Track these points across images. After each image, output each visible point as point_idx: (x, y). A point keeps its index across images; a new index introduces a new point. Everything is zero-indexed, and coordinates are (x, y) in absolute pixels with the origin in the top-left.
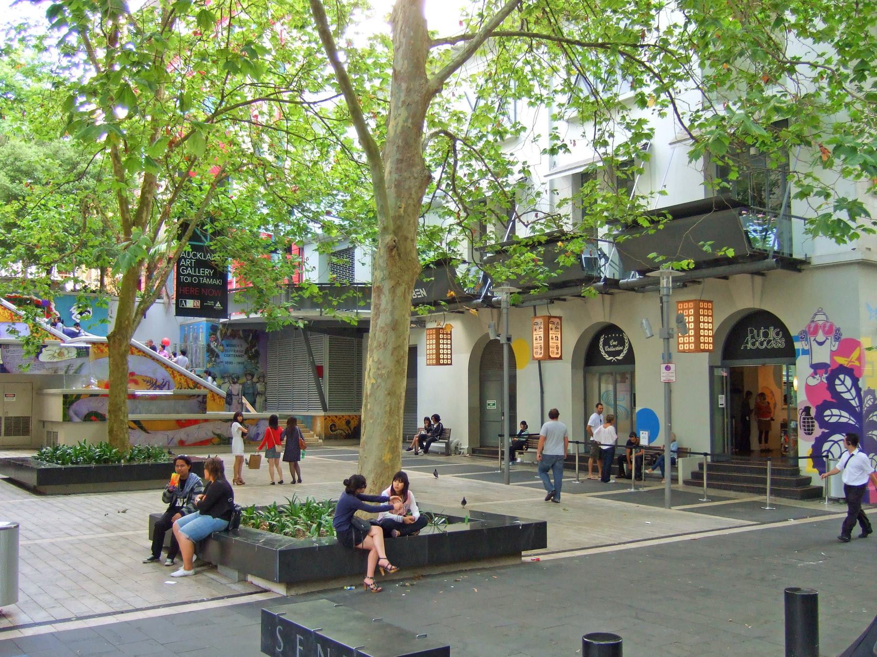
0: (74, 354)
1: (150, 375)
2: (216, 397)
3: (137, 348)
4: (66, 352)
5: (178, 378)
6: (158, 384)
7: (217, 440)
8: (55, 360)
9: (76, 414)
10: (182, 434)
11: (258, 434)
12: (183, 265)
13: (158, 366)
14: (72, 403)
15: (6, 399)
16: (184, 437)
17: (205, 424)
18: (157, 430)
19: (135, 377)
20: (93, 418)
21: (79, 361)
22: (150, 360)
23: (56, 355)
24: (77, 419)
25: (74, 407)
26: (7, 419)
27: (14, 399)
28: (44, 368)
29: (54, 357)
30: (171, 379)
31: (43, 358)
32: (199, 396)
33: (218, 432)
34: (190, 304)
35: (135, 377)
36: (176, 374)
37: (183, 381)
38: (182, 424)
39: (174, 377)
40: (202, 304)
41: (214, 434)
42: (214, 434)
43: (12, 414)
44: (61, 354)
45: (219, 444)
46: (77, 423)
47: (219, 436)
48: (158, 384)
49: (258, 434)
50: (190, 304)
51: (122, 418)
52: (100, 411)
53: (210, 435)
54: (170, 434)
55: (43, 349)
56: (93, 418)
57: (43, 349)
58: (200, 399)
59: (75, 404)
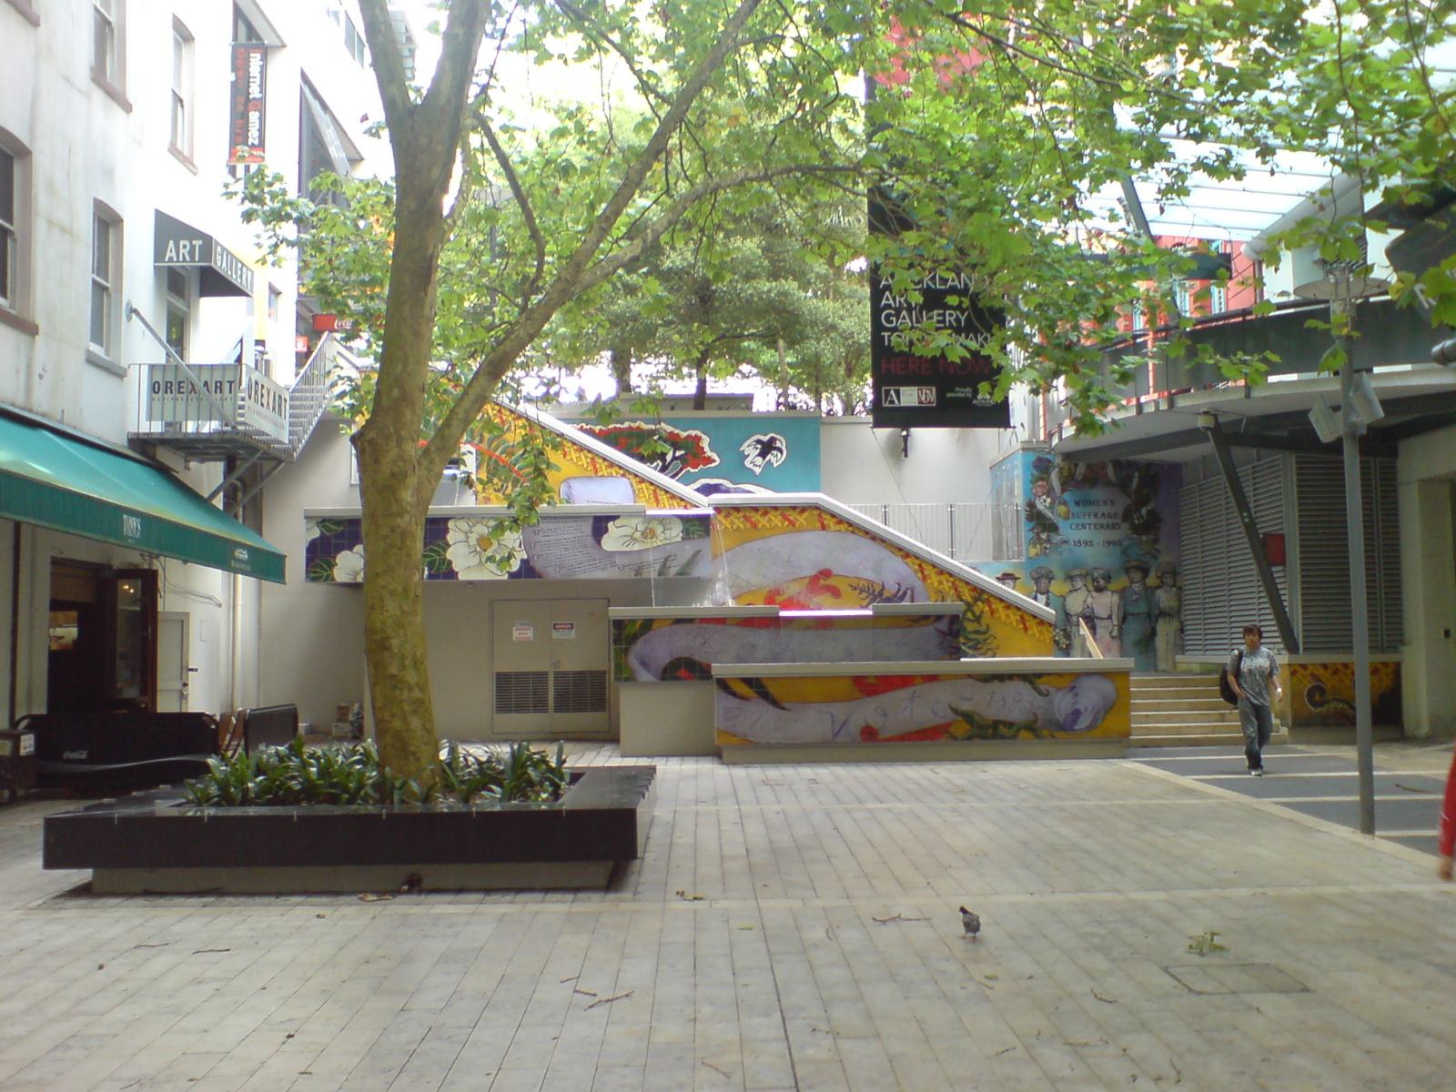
0: (676, 532)
1: (869, 575)
2: (1031, 623)
3: (833, 515)
4: (659, 529)
5: (934, 579)
6: (886, 594)
7: (962, 728)
8: (636, 547)
9: (644, 664)
10: (867, 711)
11: (1076, 714)
12: (888, 306)
13: (884, 553)
14: (634, 639)
15: (556, 635)
16: (875, 721)
17: (927, 686)
18: (805, 701)
19: (831, 582)
20: (682, 672)
21: (690, 548)
22: (867, 542)
23: (638, 535)
24: (644, 676)
25: (639, 647)
26: (560, 676)
27: (573, 634)
28: (613, 564)
29: (633, 539)
30: (918, 584)
31: (611, 542)
32: (939, 618)
33: (965, 706)
34: (910, 396)
35: (831, 582)
36: (929, 570)
37: (946, 586)
38: (868, 687)
39: (924, 578)
40: (940, 395)
41: (955, 711)
42: (955, 711)
43: (570, 665)
44: (649, 534)
45: (970, 738)
46: (647, 684)
47: (968, 717)
48: (886, 594)
49: (1076, 714)
50: (910, 396)
51: (393, 670)
52: (696, 658)
53: (944, 715)
54: (839, 710)
55: (610, 525)
56: (682, 672)
57: (610, 525)
58: (943, 626)
59: (640, 642)
